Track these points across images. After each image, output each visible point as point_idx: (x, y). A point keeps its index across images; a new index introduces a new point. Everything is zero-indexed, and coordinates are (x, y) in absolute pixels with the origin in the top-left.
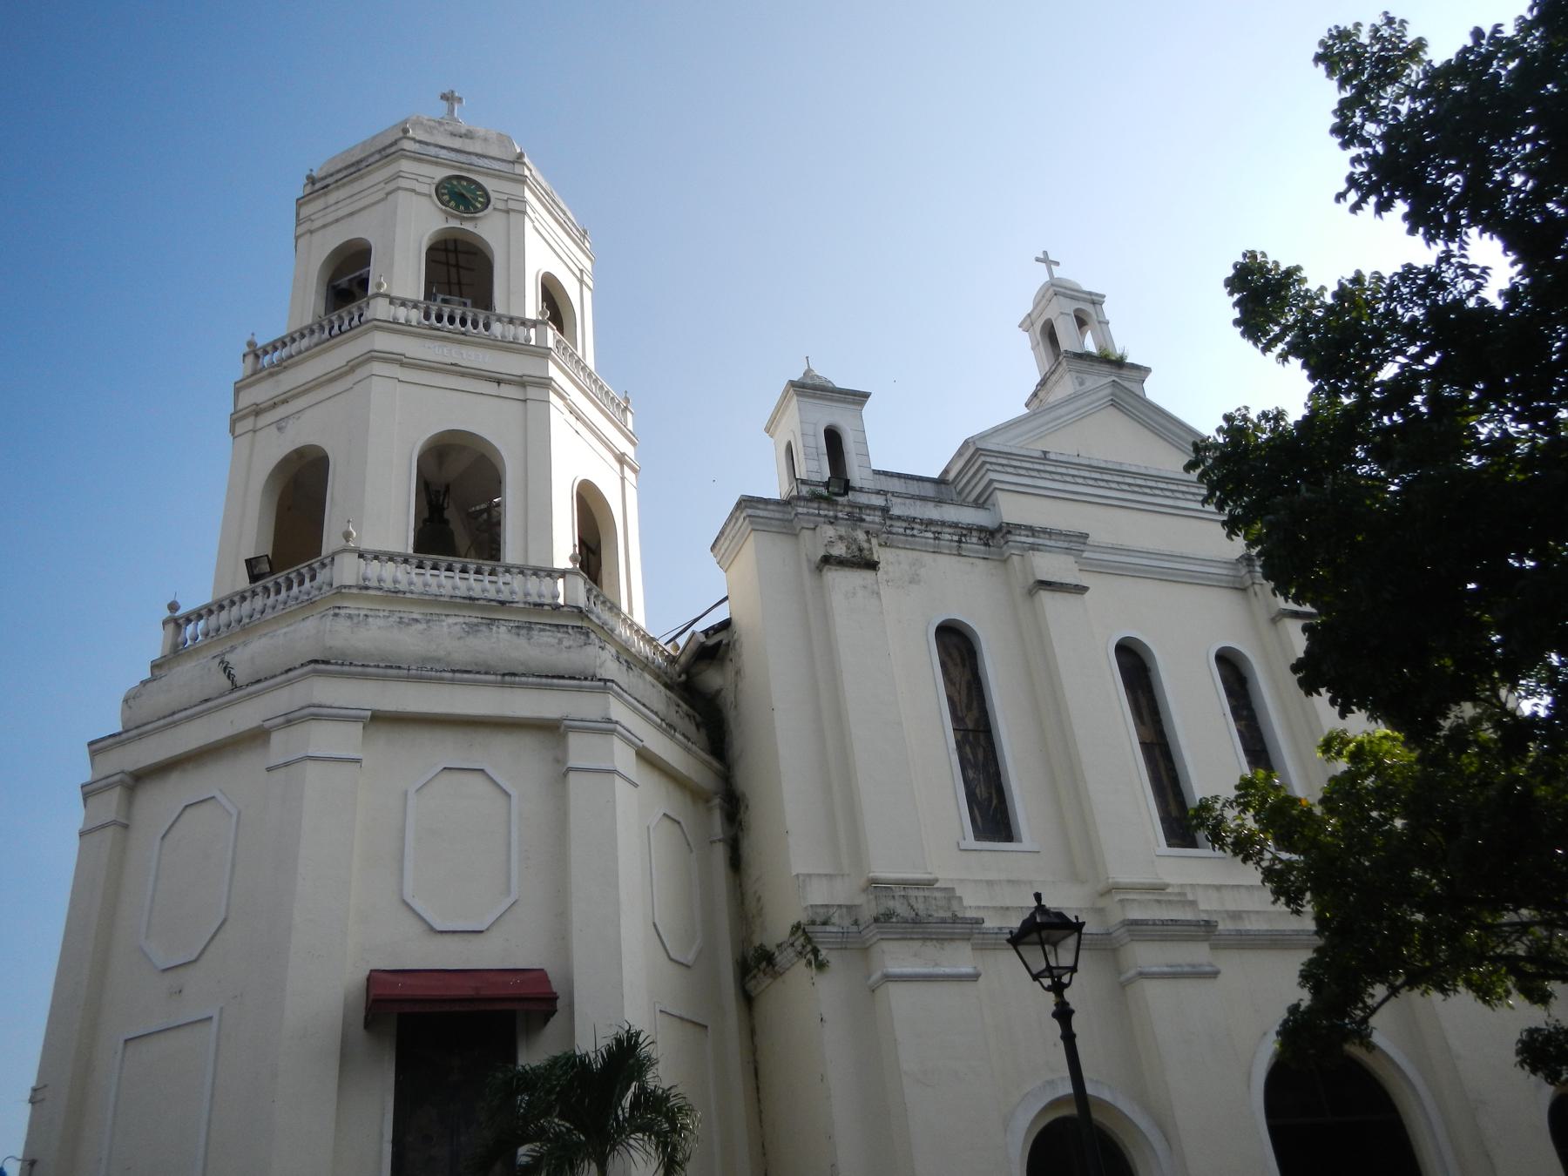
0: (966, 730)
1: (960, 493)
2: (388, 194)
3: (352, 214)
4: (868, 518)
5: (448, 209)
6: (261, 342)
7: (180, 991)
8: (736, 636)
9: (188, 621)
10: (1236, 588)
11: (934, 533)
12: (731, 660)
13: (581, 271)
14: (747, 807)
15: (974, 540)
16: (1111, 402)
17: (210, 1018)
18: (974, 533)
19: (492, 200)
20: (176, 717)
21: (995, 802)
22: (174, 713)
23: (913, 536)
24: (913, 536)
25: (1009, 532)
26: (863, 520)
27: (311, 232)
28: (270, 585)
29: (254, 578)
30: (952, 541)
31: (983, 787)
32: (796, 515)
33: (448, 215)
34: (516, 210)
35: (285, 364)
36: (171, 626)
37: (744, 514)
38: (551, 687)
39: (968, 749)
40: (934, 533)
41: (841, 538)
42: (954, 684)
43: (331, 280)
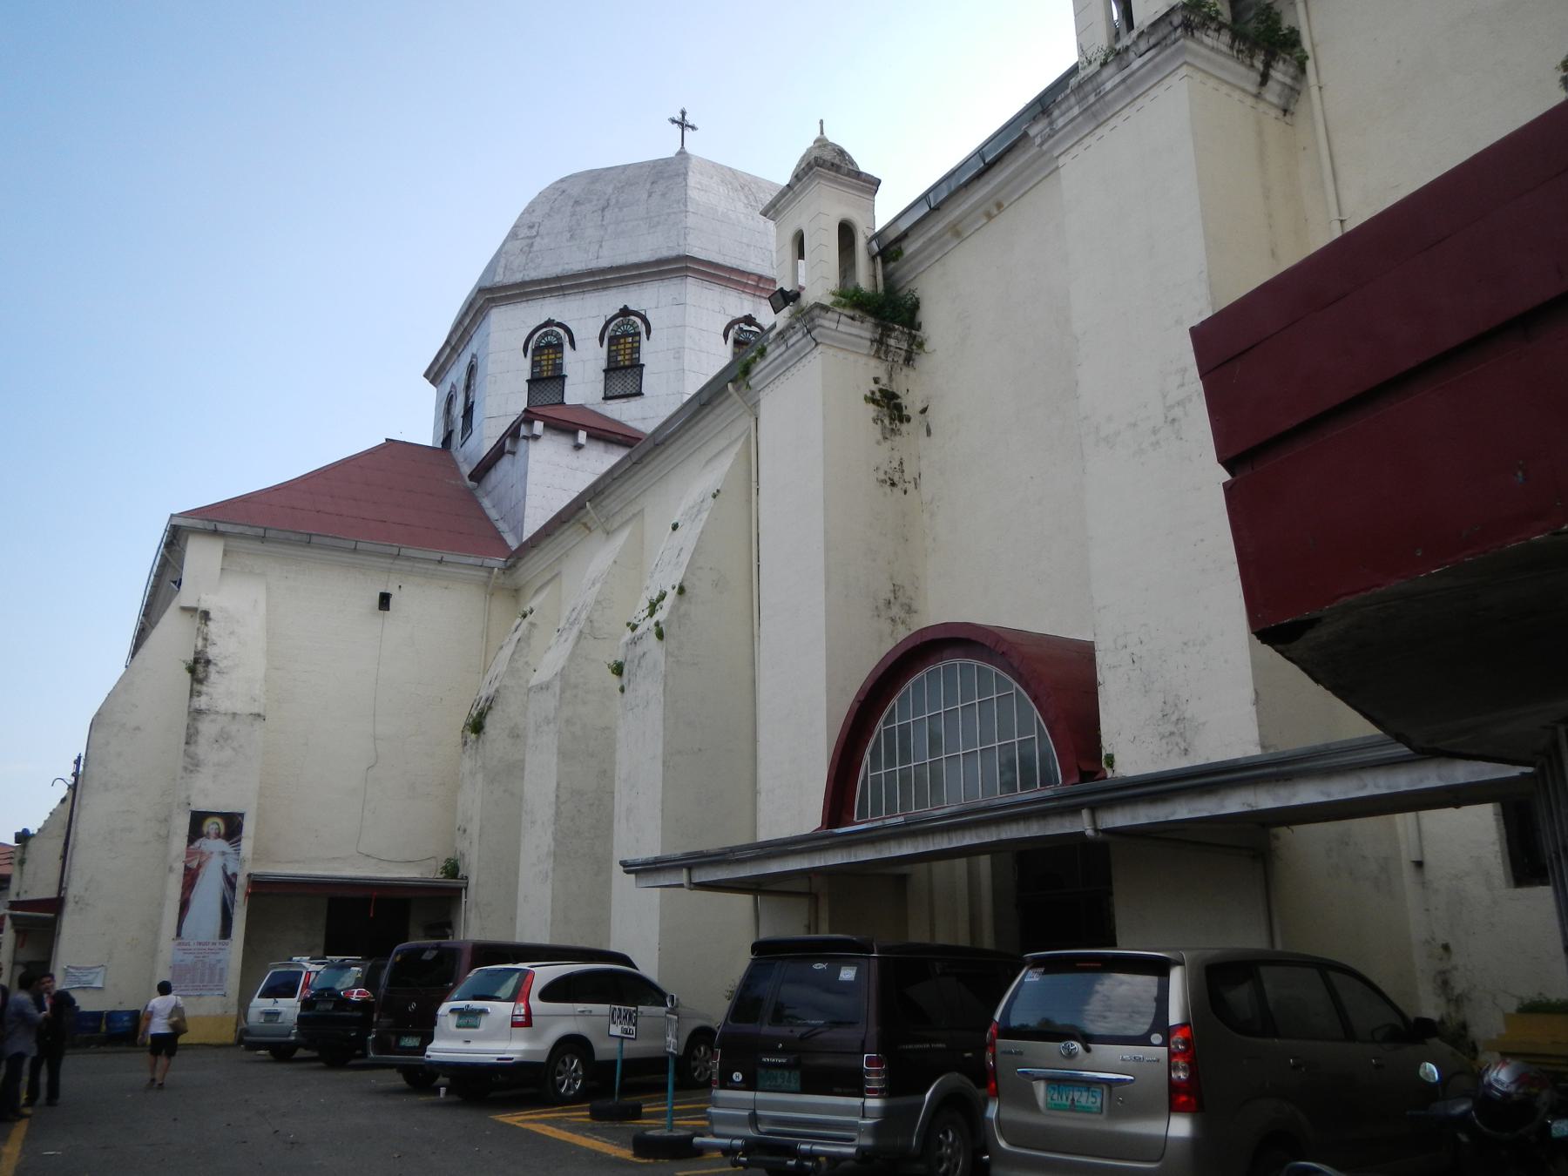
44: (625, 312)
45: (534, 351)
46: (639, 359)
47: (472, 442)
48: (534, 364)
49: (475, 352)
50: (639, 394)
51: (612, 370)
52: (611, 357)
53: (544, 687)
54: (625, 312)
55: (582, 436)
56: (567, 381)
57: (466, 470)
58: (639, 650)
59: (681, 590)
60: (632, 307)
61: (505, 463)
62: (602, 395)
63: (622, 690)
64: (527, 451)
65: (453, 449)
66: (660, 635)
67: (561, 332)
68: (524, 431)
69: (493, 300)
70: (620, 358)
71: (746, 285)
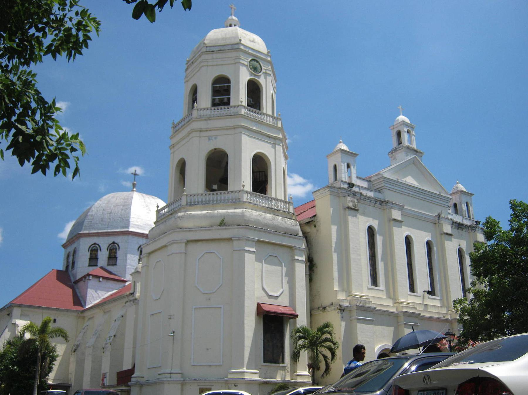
1: (373, 185)
4: (357, 195)
7: (210, 299)
8: (318, 220)
10: (433, 223)
11: (370, 200)
12: (315, 226)
14: (317, 267)
15: (379, 203)
17: (221, 307)
18: (379, 201)
19: (263, 69)
20: (202, 229)
22: (202, 228)
23: (365, 200)
24: (365, 200)
25: (387, 203)
26: (356, 196)
27: (207, 66)
30: (373, 203)
32: (341, 192)
33: (251, 74)
35: (210, 118)
37: (329, 190)
38: (292, 238)
40: (370, 200)
41: (351, 201)
44: (114, 243)
45: (91, 251)
46: (116, 256)
47: (74, 271)
48: (91, 254)
49: (76, 246)
50: (116, 265)
51: (110, 258)
52: (110, 254)
53: (89, 347)
54: (114, 243)
55: (101, 280)
56: (99, 259)
57: (73, 281)
58: (107, 346)
59: (115, 336)
60: (116, 242)
61: (82, 283)
62: (107, 264)
63: (103, 352)
64: (88, 282)
65: (69, 270)
66: (110, 344)
67: (98, 246)
68: (87, 278)
69: (81, 236)
70: (112, 255)
71: (144, 236)
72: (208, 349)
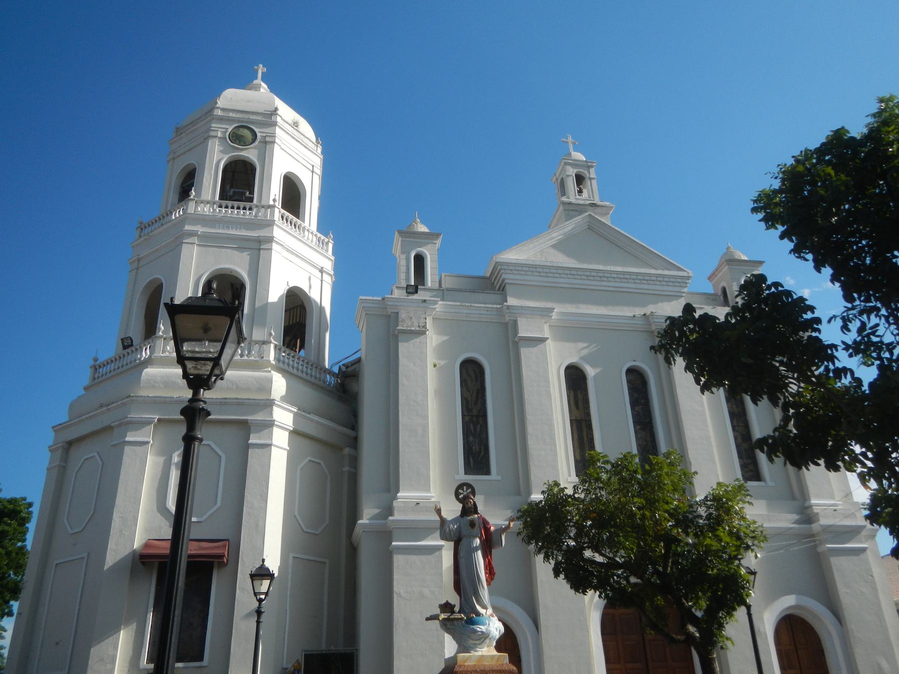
0: (473, 416)
2: (205, 139)
3: (190, 150)
5: (235, 145)
6: (145, 221)
9: (100, 367)
13: (313, 166)
16: (588, 227)
17: (84, 557)
21: (482, 453)
28: (130, 351)
29: (125, 348)
31: (477, 446)
34: (268, 143)
36: (93, 369)
39: (472, 426)
42: (469, 391)
43: (183, 183)
72: (57, 644)
